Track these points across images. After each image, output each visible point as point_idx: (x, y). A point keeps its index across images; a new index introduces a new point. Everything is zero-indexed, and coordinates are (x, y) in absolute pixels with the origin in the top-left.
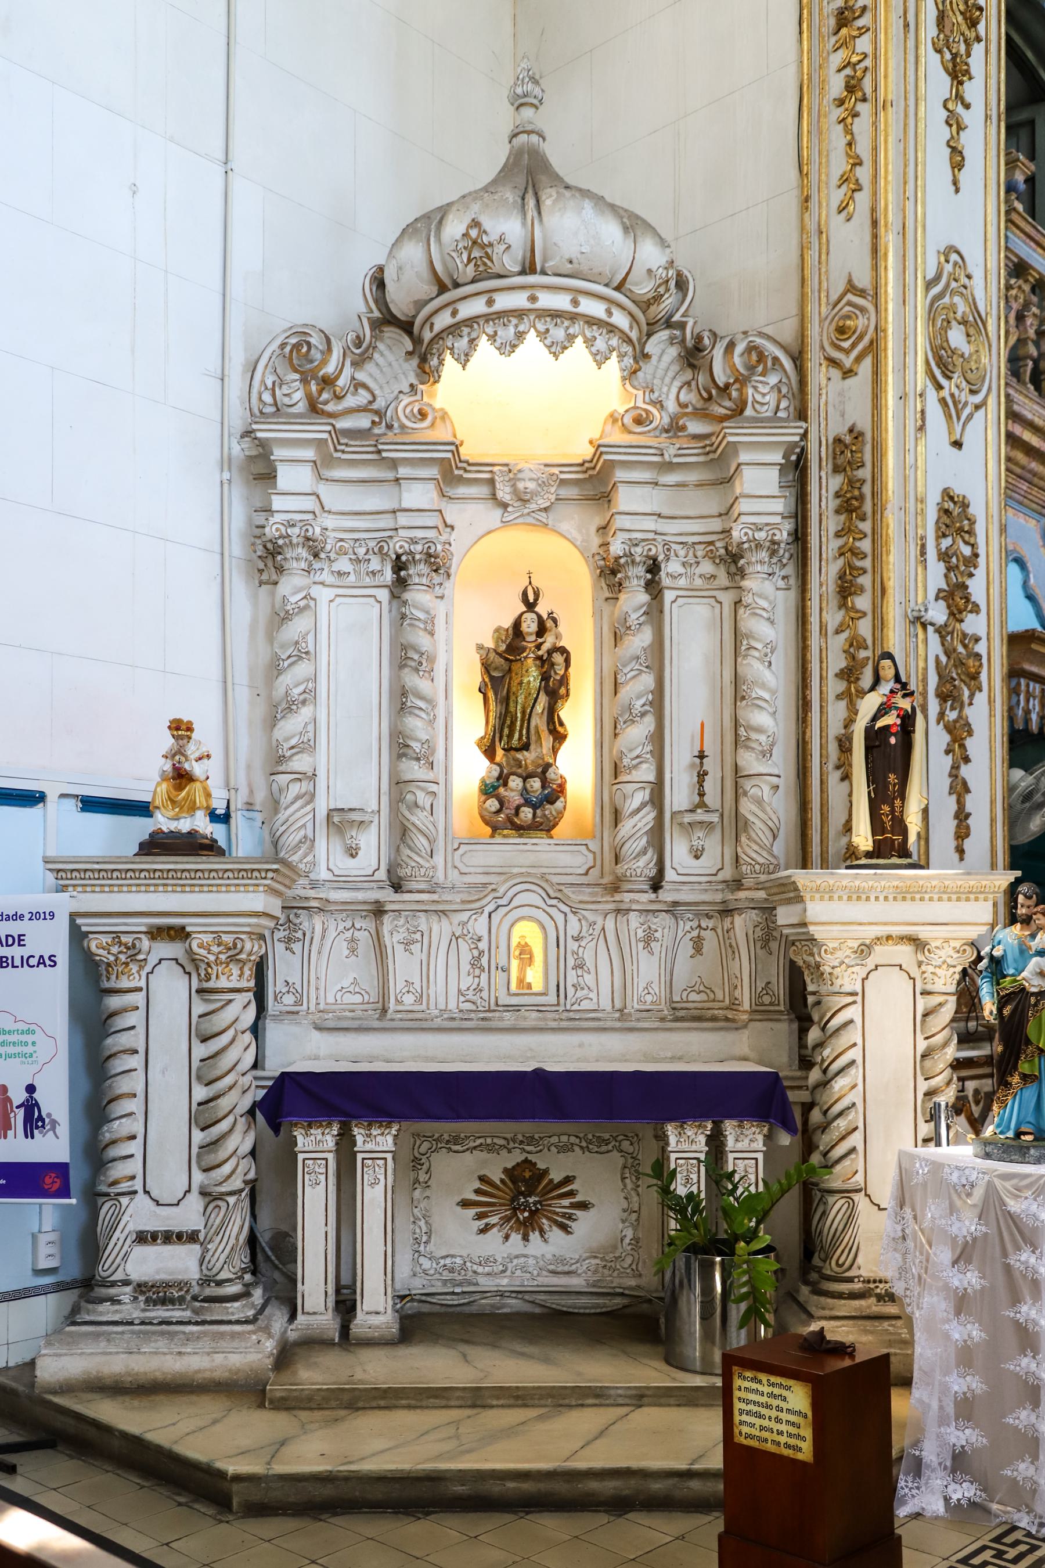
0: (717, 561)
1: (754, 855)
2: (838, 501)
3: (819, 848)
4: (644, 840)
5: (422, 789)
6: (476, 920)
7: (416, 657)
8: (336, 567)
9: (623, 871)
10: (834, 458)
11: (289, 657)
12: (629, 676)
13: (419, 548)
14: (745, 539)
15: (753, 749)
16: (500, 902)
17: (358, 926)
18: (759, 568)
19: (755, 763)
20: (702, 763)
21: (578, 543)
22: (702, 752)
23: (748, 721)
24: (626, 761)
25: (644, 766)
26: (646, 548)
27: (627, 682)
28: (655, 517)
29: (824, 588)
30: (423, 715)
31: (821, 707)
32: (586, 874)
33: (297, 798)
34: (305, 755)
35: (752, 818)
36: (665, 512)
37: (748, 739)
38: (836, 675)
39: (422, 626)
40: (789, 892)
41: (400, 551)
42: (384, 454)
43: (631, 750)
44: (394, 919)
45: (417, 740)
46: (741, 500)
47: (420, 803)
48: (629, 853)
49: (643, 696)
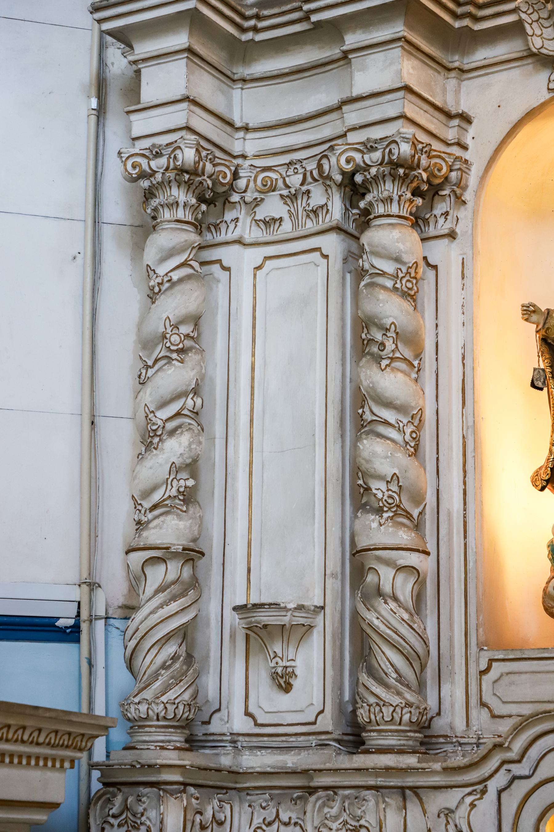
5: (388, 563)
6: (473, 805)
7: (378, 336)
8: (262, 213)
11: (156, 361)
13: (377, 156)
16: (517, 770)
17: (284, 817)
30: (393, 434)
33: (161, 589)
34: (169, 518)
39: (389, 284)
40: (434, 773)
41: (349, 168)
42: (314, 18)
44: (324, 805)
45: (381, 478)
47: (387, 588)
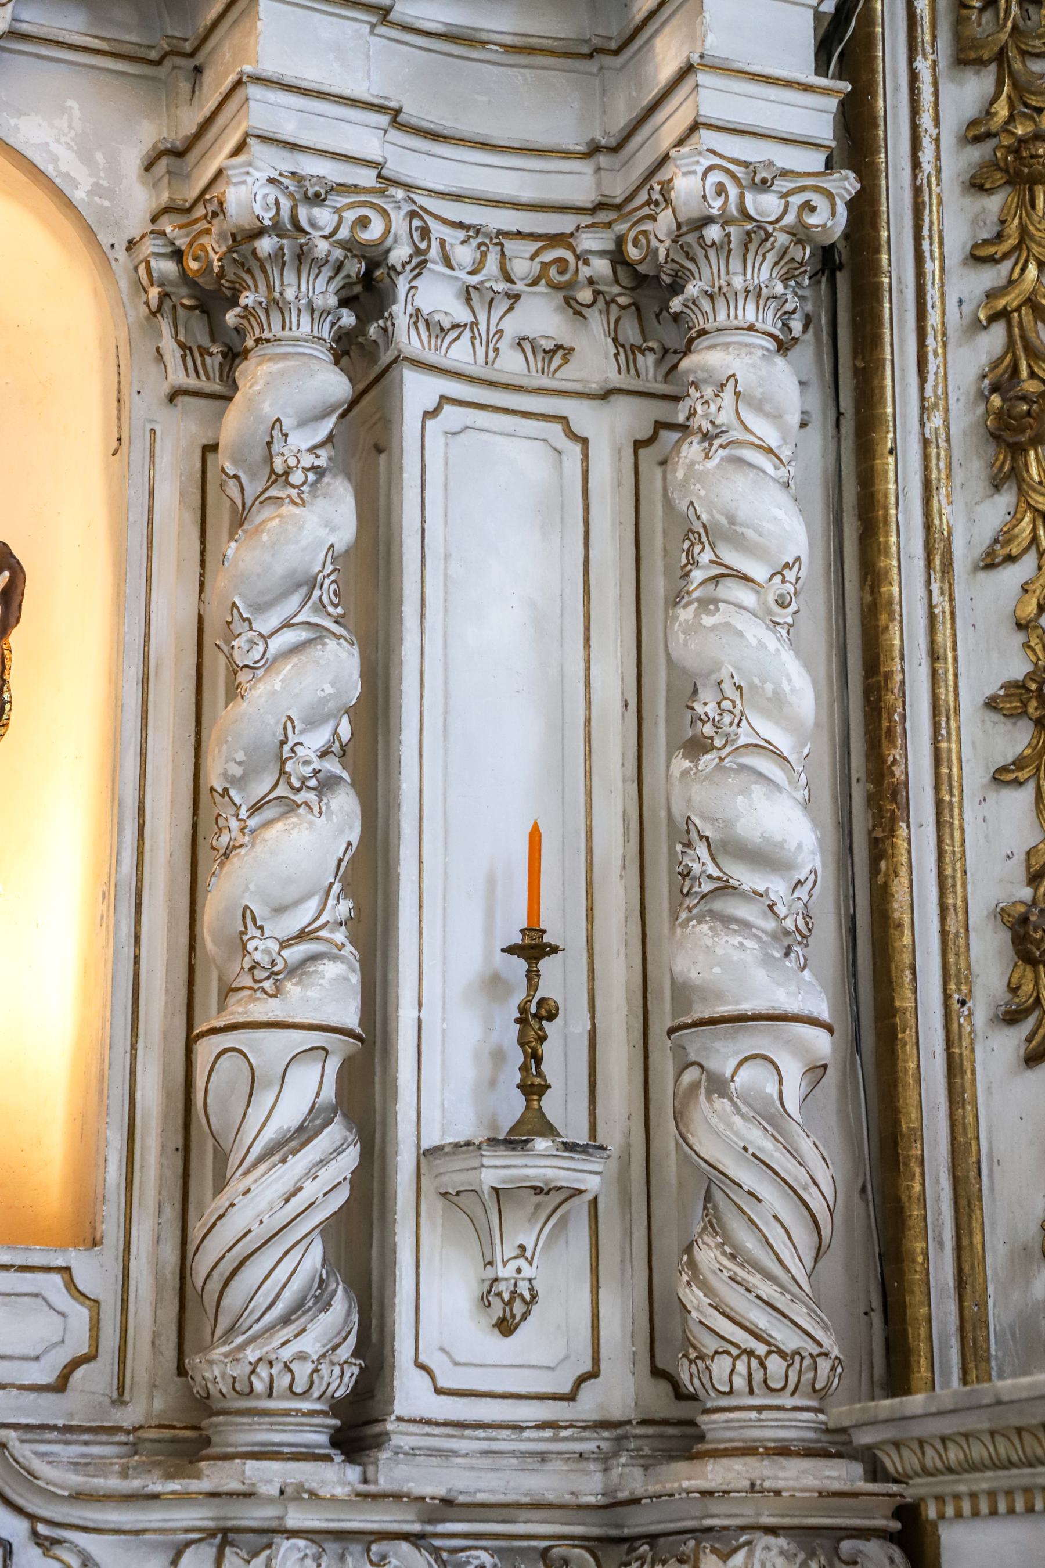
0: (585, 295)
1: (762, 1319)
2: (976, 154)
3: (952, 1307)
4: (317, 1251)
9: (240, 1371)
10: (959, 22)
12: (276, 644)
14: (716, 205)
15: (746, 925)
18: (749, 314)
19: (760, 975)
20: (533, 976)
21: (79, 196)
22: (534, 930)
23: (729, 824)
24: (261, 949)
25: (330, 970)
26: (350, 216)
27: (269, 664)
28: (384, 120)
29: (936, 421)
31: (939, 803)
32: (61, 1385)
35: (748, 1177)
36: (414, 111)
37: (725, 888)
38: (991, 704)
43: (280, 910)
46: (702, 78)
48: (262, 1300)
49: (324, 720)
